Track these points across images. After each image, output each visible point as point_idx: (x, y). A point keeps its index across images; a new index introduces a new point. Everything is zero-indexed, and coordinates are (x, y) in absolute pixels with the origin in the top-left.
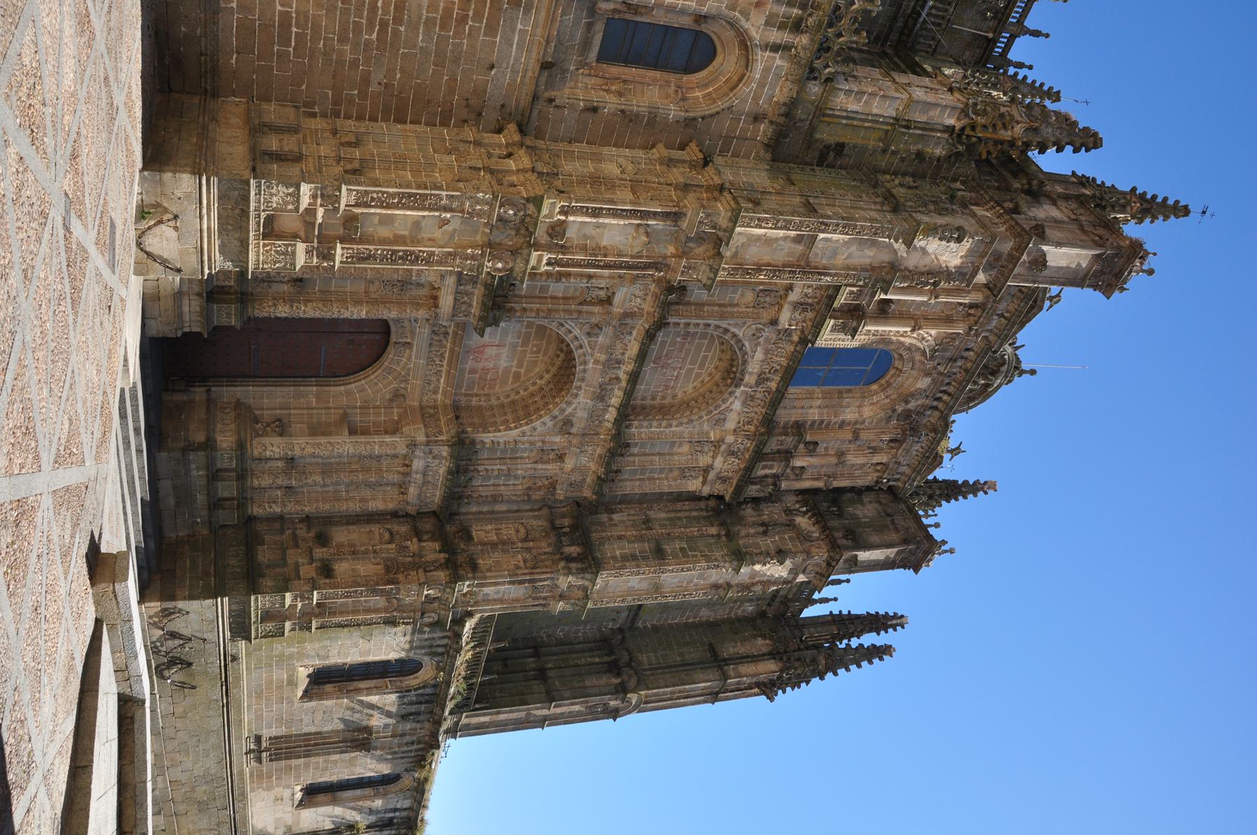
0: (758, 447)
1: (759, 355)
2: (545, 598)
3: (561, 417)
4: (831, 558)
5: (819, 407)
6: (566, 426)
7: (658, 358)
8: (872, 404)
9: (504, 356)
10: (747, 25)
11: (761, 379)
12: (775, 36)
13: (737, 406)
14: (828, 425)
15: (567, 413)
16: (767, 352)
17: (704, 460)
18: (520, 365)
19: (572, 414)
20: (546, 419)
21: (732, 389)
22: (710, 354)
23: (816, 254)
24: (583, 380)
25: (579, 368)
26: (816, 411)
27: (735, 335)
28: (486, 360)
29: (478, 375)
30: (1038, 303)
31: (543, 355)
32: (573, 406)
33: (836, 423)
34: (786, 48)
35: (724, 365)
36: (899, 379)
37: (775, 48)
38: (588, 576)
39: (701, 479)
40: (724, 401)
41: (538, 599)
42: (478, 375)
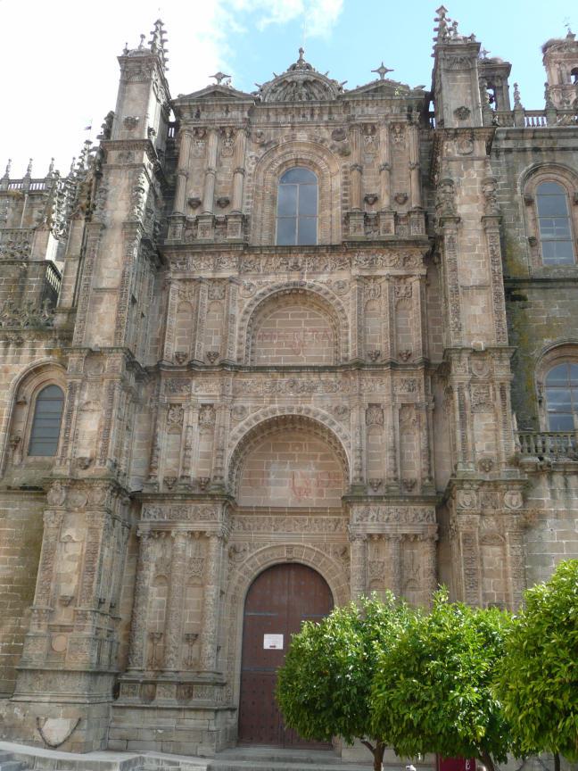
0: (359, 245)
1: (271, 278)
2: (494, 390)
3: (331, 417)
4: (447, 137)
5: (331, 209)
6: (341, 412)
7: (294, 352)
8: (329, 168)
9: (303, 471)
10: (19, 374)
11: (296, 267)
12: (26, 354)
13: (324, 278)
14: (345, 195)
15: (327, 413)
16: (267, 274)
17: (385, 285)
18: (315, 457)
19: (329, 409)
20: (334, 429)
21: (306, 288)
22: (290, 313)
23: (113, 283)
24: (291, 409)
25: (278, 414)
26: (335, 210)
27: (251, 305)
28: (307, 485)
29: (325, 489)
30: (212, 91)
31: (304, 440)
32: (319, 409)
33: (345, 189)
34: (33, 345)
35: (291, 299)
36: (303, 157)
37: (33, 352)
38: (455, 356)
39: (411, 280)
40: (320, 289)
41: (495, 395)
42: (325, 489)
